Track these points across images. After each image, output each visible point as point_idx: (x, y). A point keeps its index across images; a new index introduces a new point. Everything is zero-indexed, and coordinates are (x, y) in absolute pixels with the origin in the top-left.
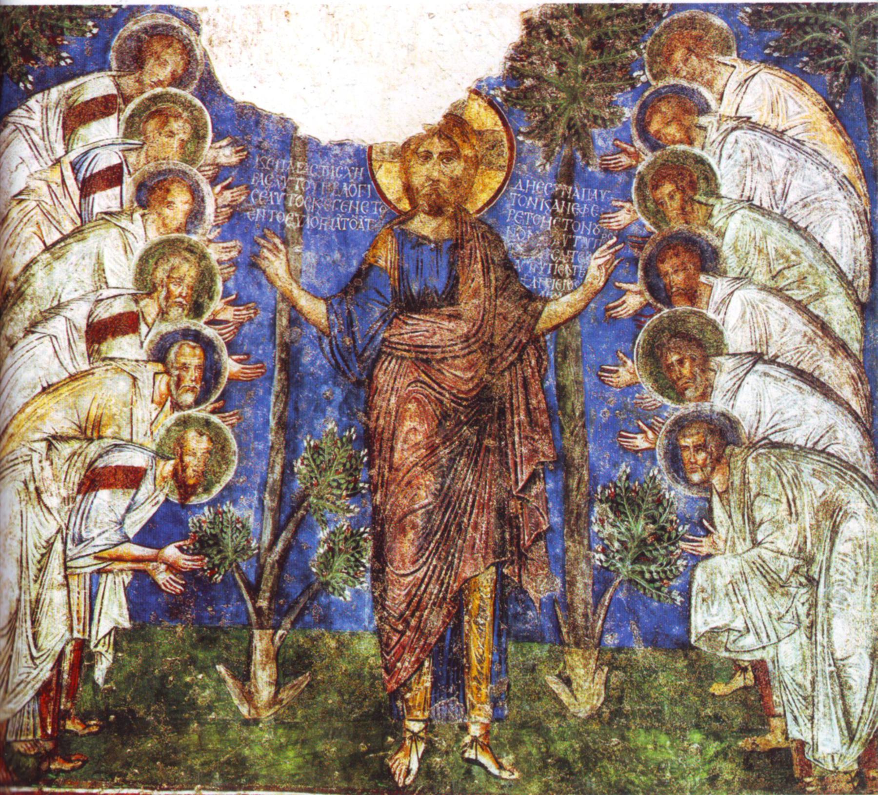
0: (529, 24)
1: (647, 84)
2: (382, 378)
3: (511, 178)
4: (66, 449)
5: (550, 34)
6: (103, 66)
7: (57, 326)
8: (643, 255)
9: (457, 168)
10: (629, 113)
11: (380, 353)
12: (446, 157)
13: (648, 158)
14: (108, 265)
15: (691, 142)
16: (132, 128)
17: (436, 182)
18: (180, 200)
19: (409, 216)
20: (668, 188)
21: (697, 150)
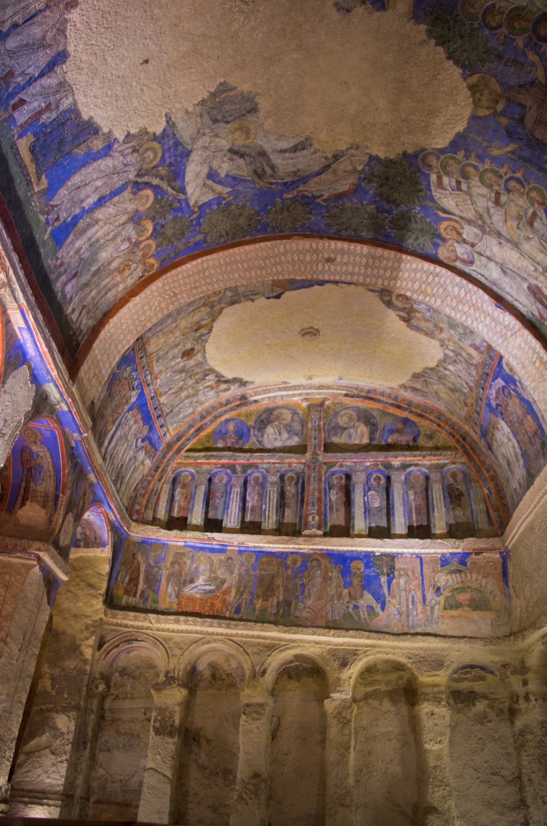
0: (449, 58)
1: (479, 24)
2: (539, 137)
3: (495, 76)
4: (521, 225)
5: (454, 52)
6: (429, 175)
7: (492, 211)
8: (535, 40)
9: (486, 92)
10: (487, 32)
11: (532, 134)
12: (482, 94)
13: (504, 30)
14: (481, 193)
15: (504, 13)
16: (447, 174)
17: (488, 99)
18: (470, 169)
19: (496, 111)
20: (516, 24)
21: (507, 11)
